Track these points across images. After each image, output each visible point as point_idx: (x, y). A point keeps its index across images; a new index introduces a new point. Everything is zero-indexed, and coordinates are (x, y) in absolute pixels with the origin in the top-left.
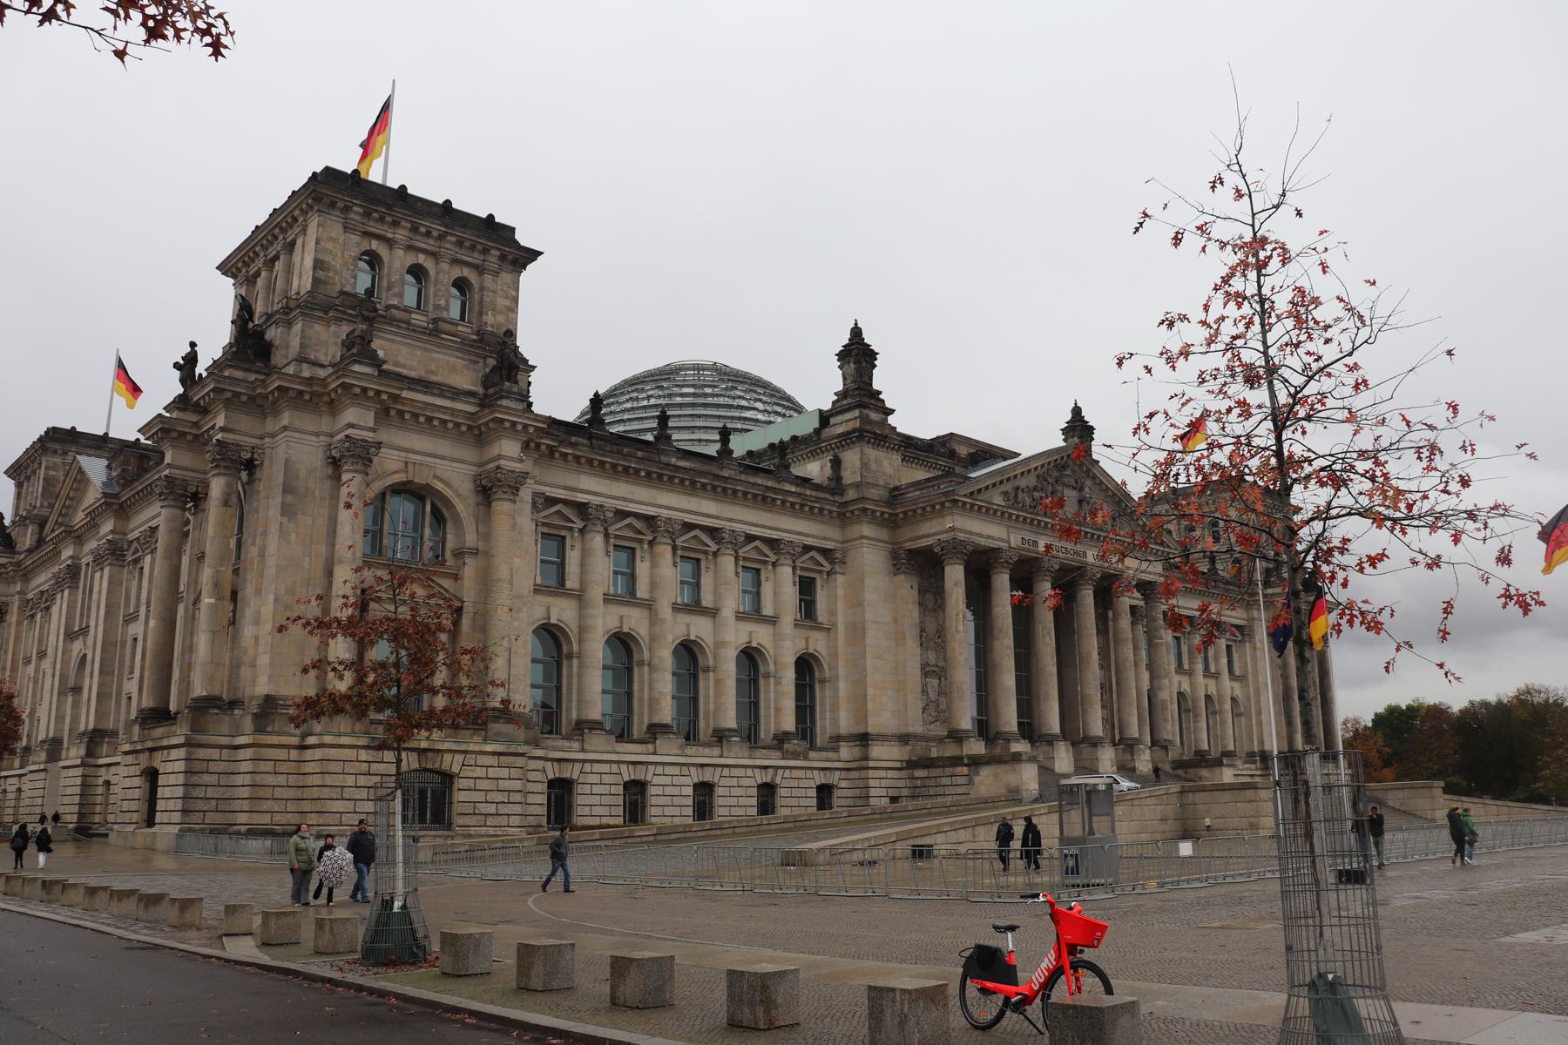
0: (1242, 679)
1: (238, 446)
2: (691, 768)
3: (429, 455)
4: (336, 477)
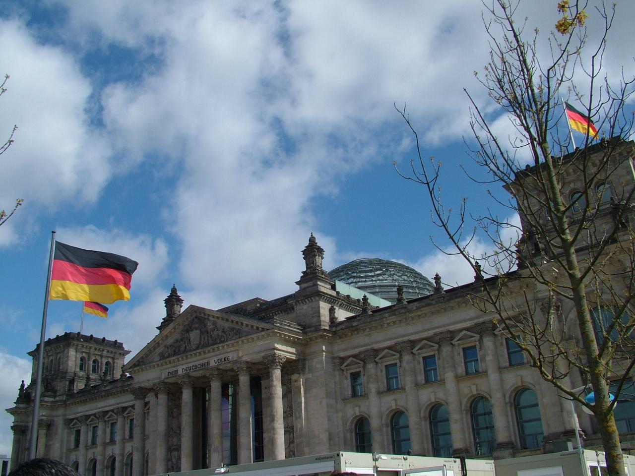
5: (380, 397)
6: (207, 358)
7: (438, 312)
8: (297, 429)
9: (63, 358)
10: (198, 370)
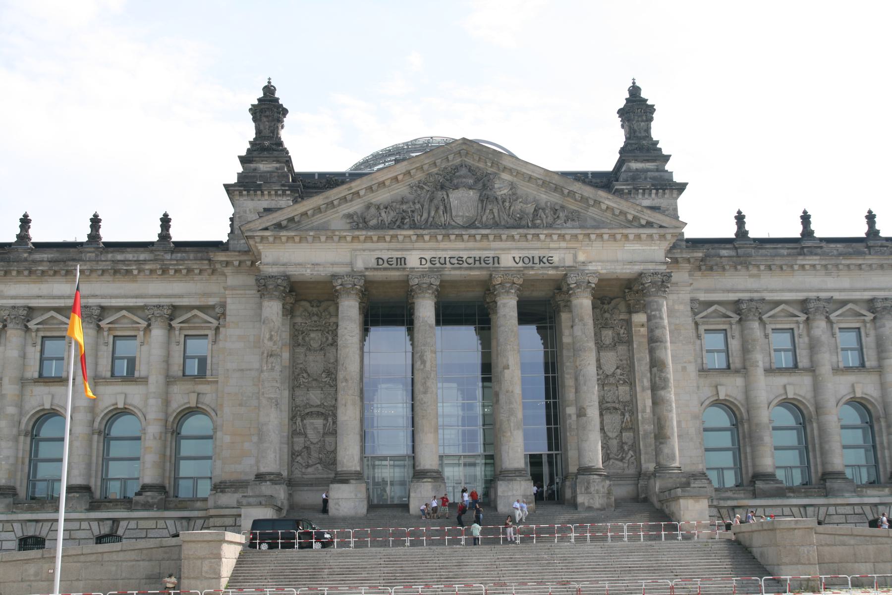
2: (14, 525)
5: (765, 376)
6: (495, 249)
8: (645, 406)
10: (470, 269)
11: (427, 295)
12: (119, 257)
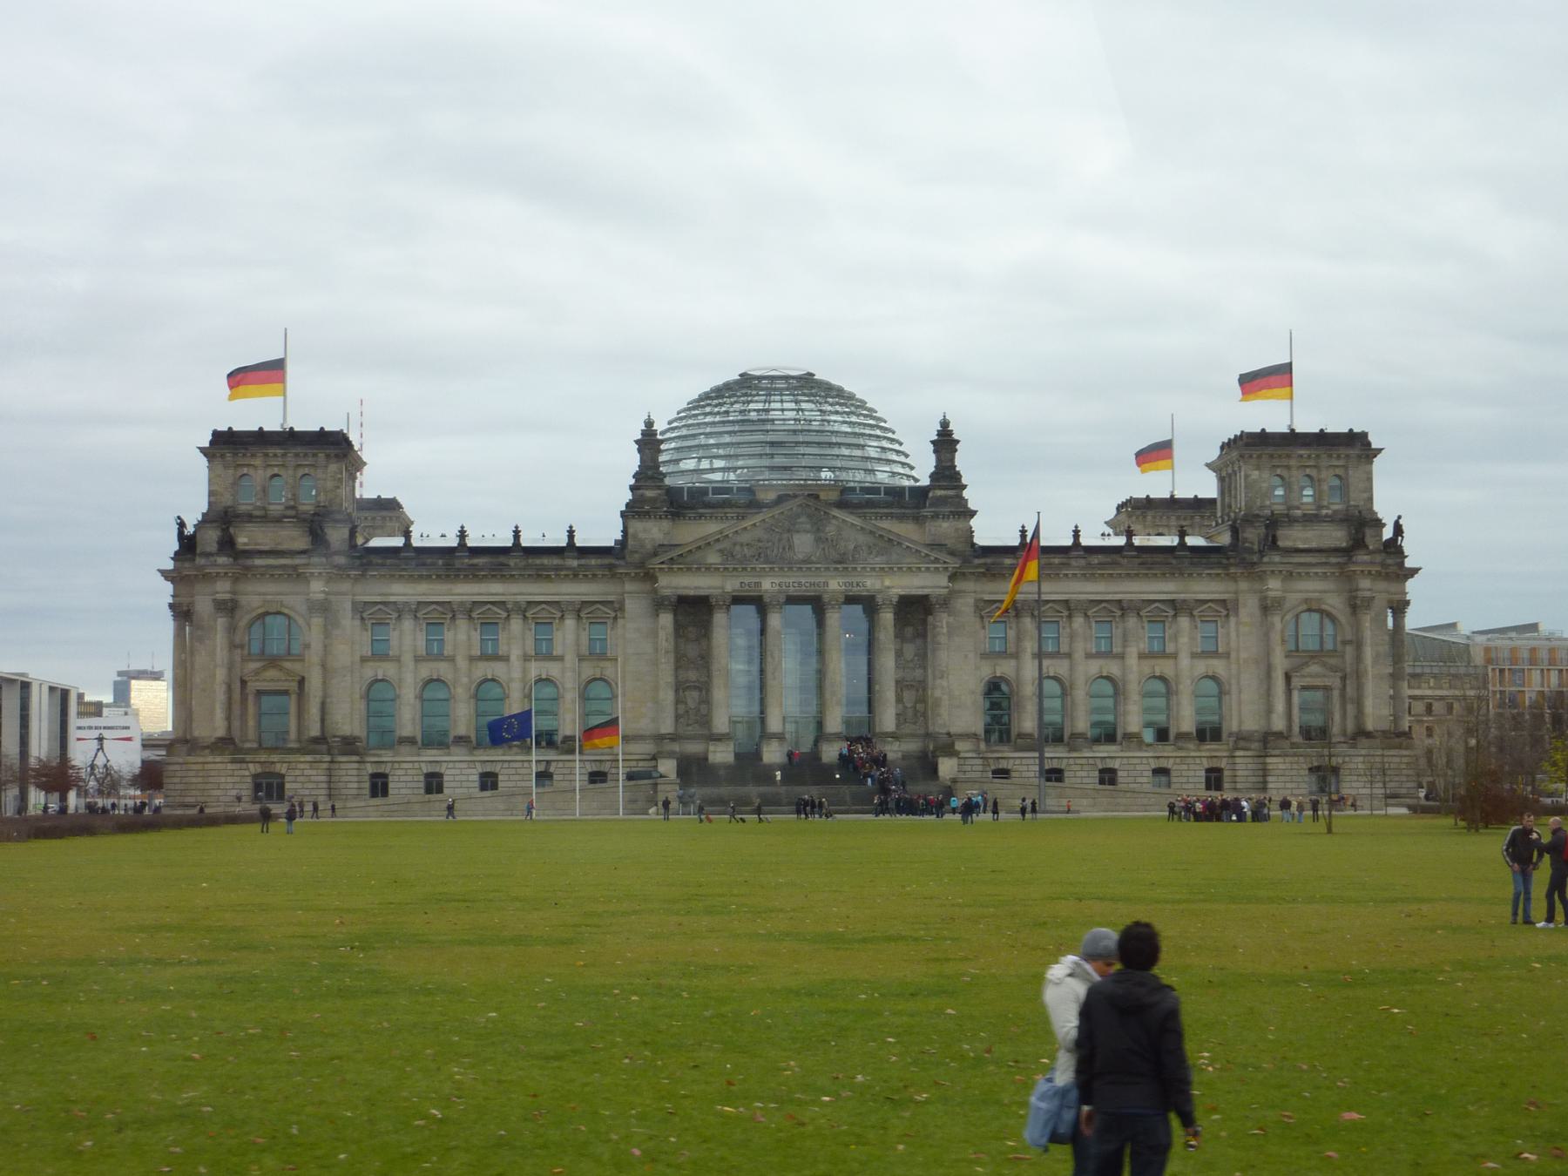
0: (1227, 655)
1: (180, 604)
2: (477, 764)
3: (278, 595)
4: (216, 621)
7: (1137, 575)
9: (325, 480)
11: (776, 610)
12: (538, 561)
